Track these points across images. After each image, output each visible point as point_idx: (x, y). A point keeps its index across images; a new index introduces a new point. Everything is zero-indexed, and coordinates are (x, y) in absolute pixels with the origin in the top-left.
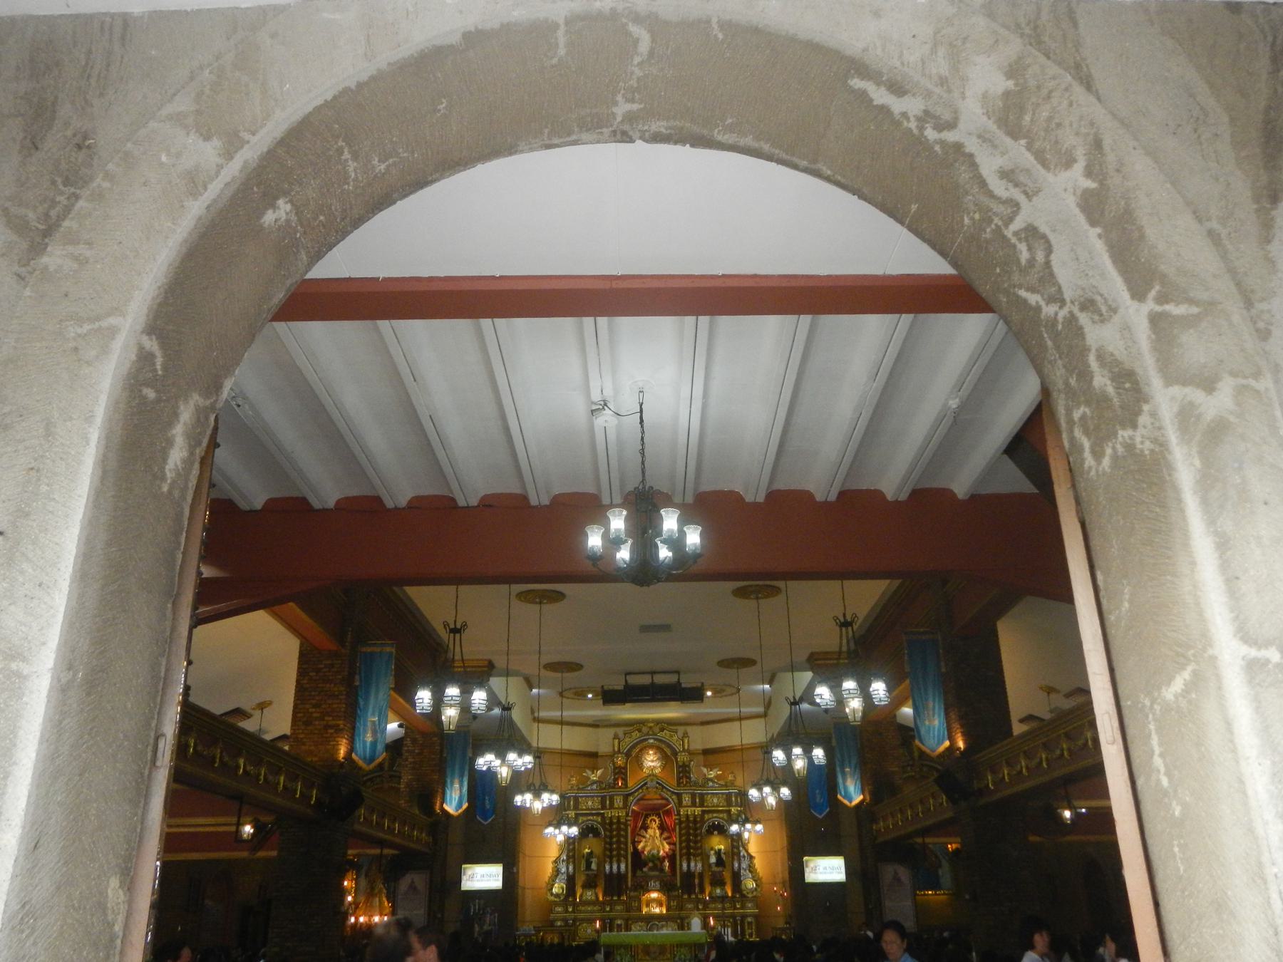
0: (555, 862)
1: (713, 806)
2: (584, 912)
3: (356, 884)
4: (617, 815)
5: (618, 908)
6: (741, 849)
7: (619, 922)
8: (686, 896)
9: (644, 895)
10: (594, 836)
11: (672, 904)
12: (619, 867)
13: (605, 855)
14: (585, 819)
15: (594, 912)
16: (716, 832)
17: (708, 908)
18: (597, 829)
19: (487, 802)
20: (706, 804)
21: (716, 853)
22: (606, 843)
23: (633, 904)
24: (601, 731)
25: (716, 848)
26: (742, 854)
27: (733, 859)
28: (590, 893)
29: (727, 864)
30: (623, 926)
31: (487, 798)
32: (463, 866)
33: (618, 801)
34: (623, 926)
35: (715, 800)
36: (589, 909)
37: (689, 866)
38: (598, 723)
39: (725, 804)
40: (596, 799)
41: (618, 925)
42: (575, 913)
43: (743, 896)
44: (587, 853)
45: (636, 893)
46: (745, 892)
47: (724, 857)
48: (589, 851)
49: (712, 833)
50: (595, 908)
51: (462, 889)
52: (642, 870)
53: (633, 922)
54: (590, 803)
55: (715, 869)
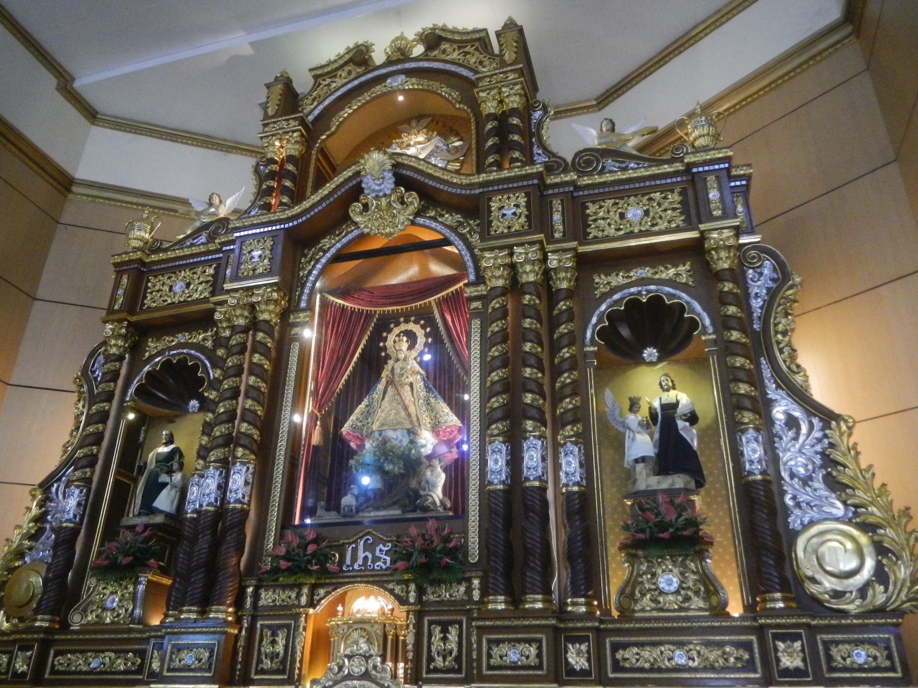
0: (46, 486)
1: (630, 235)
6: (772, 391)
8: (499, 604)
9: (312, 604)
11: (437, 644)
12: (223, 487)
16: (650, 353)
17: (617, 667)
20: (593, 232)
21: (653, 415)
25: (656, 404)
26: (778, 413)
27: (735, 429)
29: (702, 459)
33: (256, 253)
35: (634, 213)
37: (515, 461)
39: (679, 221)
43: (814, 605)
46: (813, 589)
47: (691, 435)
49: (641, 362)
54: (179, 287)
55: (647, 481)
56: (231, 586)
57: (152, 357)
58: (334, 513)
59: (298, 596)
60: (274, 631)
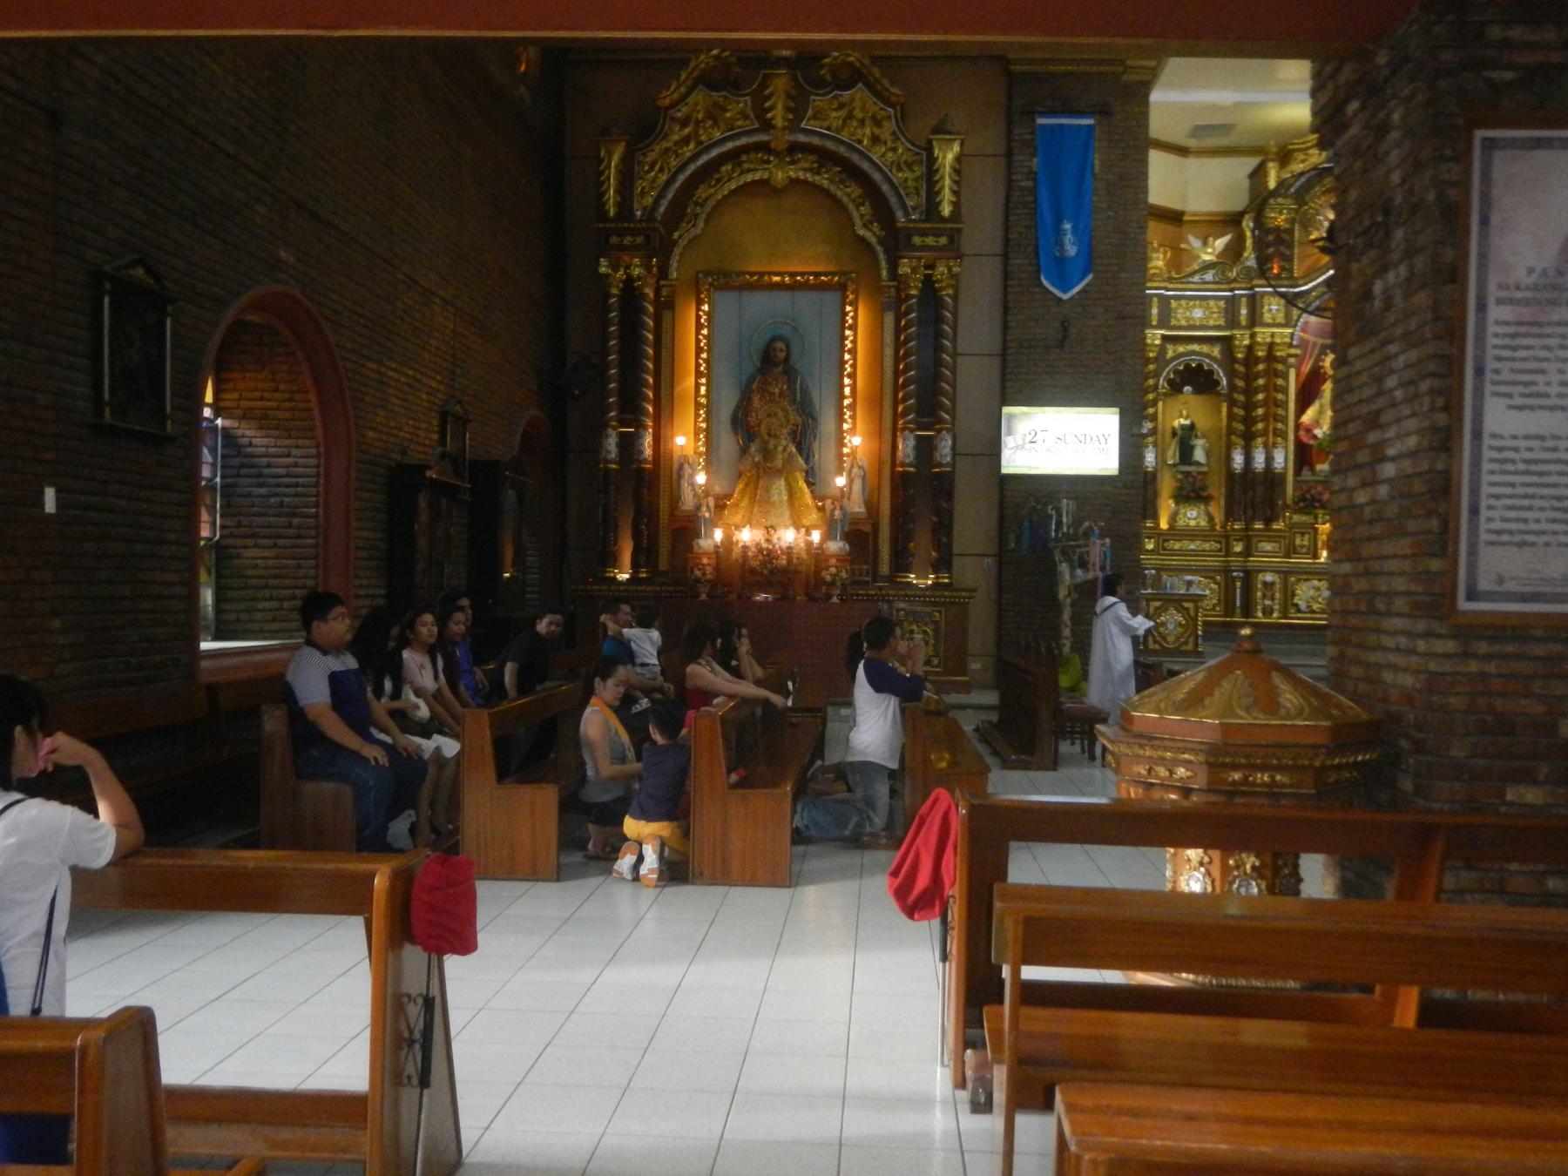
2: (1182, 553)
3: (708, 444)
4: (1269, 340)
5: (1268, 546)
7: (1269, 577)
10: (1198, 390)
12: (1269, 459)
13: (1231, 431)
14: (1181, 349)
15: (1202, 553)
18: (1211, 372)
19: (1069, 238)
22: (1232, 403)
23: (1298, 541)
24: (1193, 163)
28: (1195, 513)
30: (1278, 586)
31: (1067, 226)
32: (1006, 410)
34: (1278, 586)
36: (1192, 547)
38: (1191, 143)
40: (1212, 303)
41: (1265, 584)
42: (1159, 554)
44: (1183, 427)
45: (1304, 518)
48: (1187, 422)
50: (1207, 546)
51: (1004, 471)
52: (1312, 469)
53: (1299, 580)
56: (1281, 514)
57: (1174, 359)
58: (1310, 473)
59: (1316, 517)
60: (1303, 534)
